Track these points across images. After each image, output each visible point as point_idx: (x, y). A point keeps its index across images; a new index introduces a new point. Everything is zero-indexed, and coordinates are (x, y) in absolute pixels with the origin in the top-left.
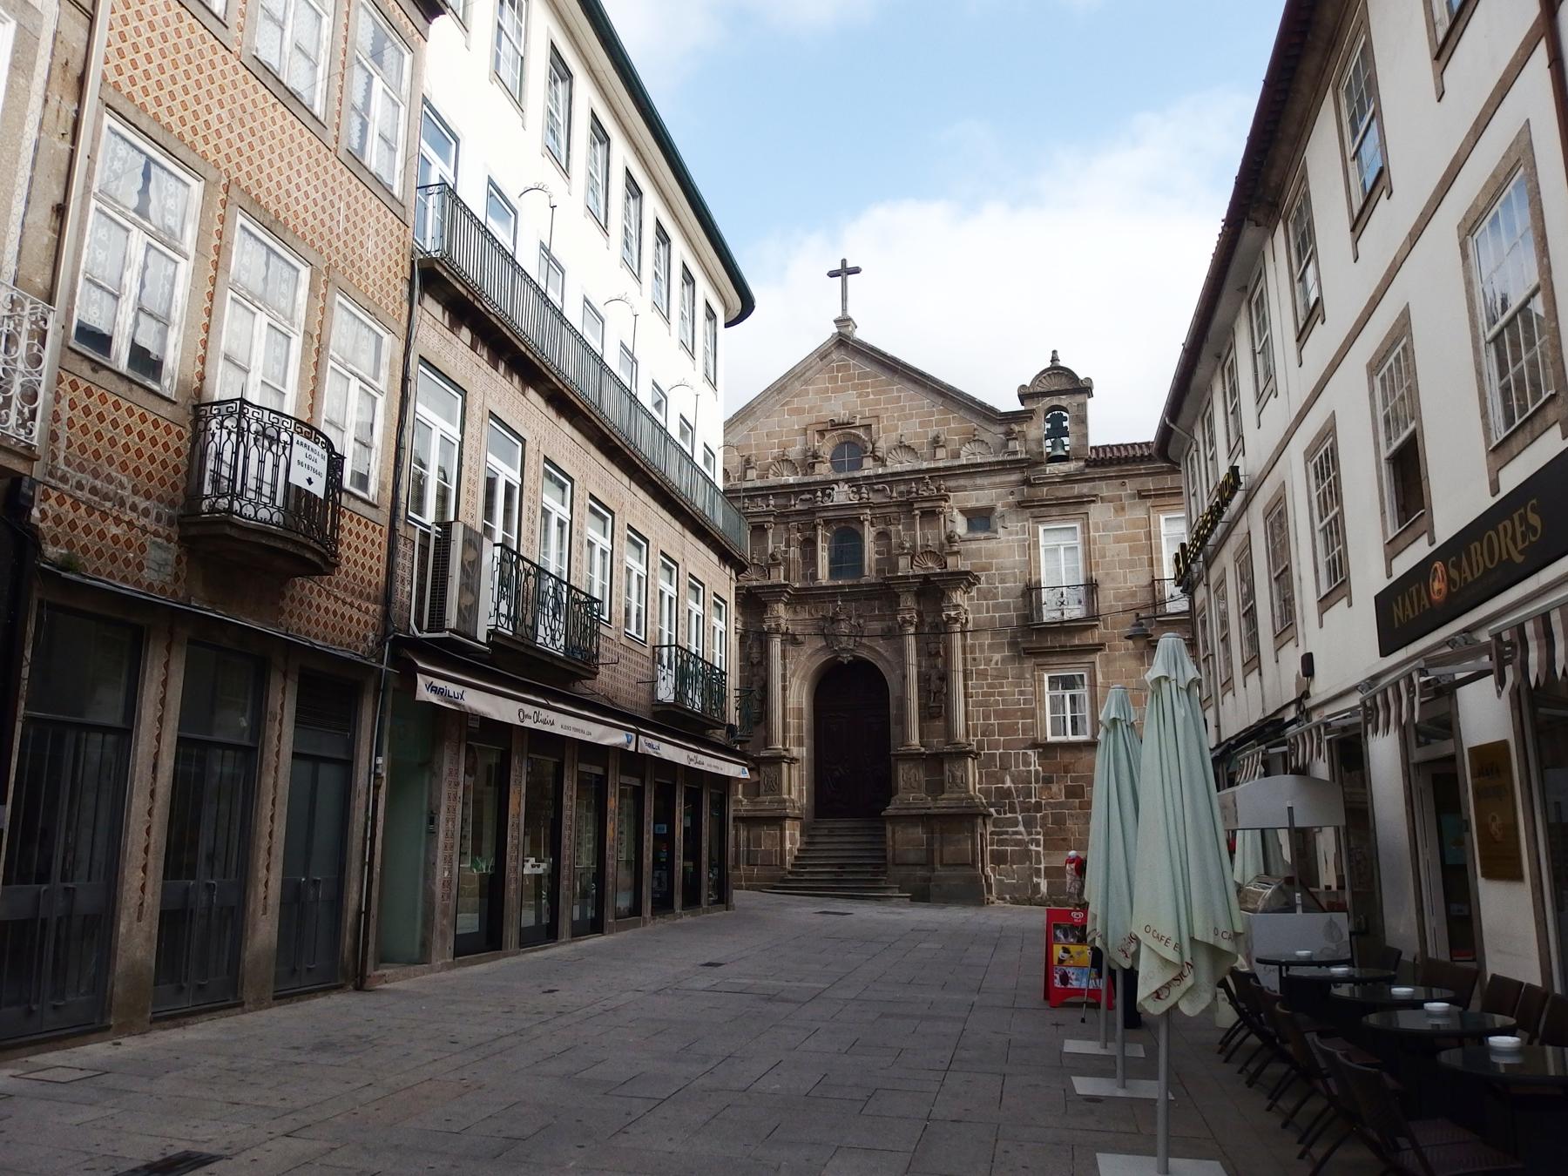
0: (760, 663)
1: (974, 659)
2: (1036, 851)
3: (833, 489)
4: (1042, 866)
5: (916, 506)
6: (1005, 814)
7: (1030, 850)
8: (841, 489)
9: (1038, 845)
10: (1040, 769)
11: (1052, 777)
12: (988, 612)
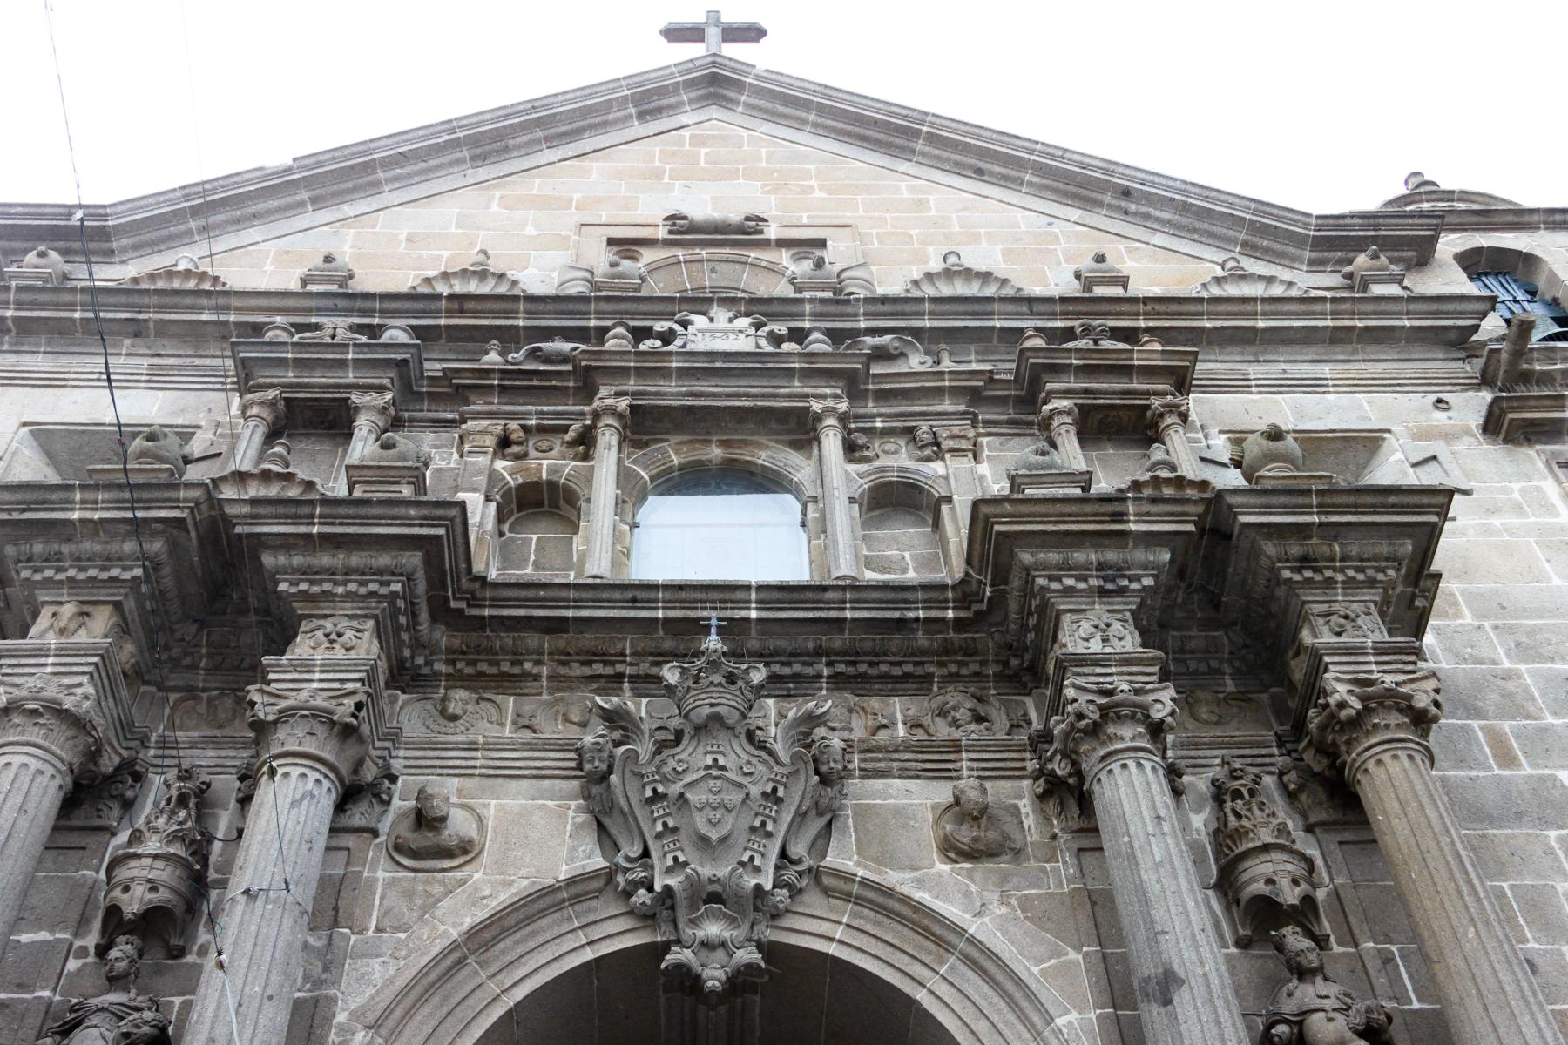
3: (685, 324)
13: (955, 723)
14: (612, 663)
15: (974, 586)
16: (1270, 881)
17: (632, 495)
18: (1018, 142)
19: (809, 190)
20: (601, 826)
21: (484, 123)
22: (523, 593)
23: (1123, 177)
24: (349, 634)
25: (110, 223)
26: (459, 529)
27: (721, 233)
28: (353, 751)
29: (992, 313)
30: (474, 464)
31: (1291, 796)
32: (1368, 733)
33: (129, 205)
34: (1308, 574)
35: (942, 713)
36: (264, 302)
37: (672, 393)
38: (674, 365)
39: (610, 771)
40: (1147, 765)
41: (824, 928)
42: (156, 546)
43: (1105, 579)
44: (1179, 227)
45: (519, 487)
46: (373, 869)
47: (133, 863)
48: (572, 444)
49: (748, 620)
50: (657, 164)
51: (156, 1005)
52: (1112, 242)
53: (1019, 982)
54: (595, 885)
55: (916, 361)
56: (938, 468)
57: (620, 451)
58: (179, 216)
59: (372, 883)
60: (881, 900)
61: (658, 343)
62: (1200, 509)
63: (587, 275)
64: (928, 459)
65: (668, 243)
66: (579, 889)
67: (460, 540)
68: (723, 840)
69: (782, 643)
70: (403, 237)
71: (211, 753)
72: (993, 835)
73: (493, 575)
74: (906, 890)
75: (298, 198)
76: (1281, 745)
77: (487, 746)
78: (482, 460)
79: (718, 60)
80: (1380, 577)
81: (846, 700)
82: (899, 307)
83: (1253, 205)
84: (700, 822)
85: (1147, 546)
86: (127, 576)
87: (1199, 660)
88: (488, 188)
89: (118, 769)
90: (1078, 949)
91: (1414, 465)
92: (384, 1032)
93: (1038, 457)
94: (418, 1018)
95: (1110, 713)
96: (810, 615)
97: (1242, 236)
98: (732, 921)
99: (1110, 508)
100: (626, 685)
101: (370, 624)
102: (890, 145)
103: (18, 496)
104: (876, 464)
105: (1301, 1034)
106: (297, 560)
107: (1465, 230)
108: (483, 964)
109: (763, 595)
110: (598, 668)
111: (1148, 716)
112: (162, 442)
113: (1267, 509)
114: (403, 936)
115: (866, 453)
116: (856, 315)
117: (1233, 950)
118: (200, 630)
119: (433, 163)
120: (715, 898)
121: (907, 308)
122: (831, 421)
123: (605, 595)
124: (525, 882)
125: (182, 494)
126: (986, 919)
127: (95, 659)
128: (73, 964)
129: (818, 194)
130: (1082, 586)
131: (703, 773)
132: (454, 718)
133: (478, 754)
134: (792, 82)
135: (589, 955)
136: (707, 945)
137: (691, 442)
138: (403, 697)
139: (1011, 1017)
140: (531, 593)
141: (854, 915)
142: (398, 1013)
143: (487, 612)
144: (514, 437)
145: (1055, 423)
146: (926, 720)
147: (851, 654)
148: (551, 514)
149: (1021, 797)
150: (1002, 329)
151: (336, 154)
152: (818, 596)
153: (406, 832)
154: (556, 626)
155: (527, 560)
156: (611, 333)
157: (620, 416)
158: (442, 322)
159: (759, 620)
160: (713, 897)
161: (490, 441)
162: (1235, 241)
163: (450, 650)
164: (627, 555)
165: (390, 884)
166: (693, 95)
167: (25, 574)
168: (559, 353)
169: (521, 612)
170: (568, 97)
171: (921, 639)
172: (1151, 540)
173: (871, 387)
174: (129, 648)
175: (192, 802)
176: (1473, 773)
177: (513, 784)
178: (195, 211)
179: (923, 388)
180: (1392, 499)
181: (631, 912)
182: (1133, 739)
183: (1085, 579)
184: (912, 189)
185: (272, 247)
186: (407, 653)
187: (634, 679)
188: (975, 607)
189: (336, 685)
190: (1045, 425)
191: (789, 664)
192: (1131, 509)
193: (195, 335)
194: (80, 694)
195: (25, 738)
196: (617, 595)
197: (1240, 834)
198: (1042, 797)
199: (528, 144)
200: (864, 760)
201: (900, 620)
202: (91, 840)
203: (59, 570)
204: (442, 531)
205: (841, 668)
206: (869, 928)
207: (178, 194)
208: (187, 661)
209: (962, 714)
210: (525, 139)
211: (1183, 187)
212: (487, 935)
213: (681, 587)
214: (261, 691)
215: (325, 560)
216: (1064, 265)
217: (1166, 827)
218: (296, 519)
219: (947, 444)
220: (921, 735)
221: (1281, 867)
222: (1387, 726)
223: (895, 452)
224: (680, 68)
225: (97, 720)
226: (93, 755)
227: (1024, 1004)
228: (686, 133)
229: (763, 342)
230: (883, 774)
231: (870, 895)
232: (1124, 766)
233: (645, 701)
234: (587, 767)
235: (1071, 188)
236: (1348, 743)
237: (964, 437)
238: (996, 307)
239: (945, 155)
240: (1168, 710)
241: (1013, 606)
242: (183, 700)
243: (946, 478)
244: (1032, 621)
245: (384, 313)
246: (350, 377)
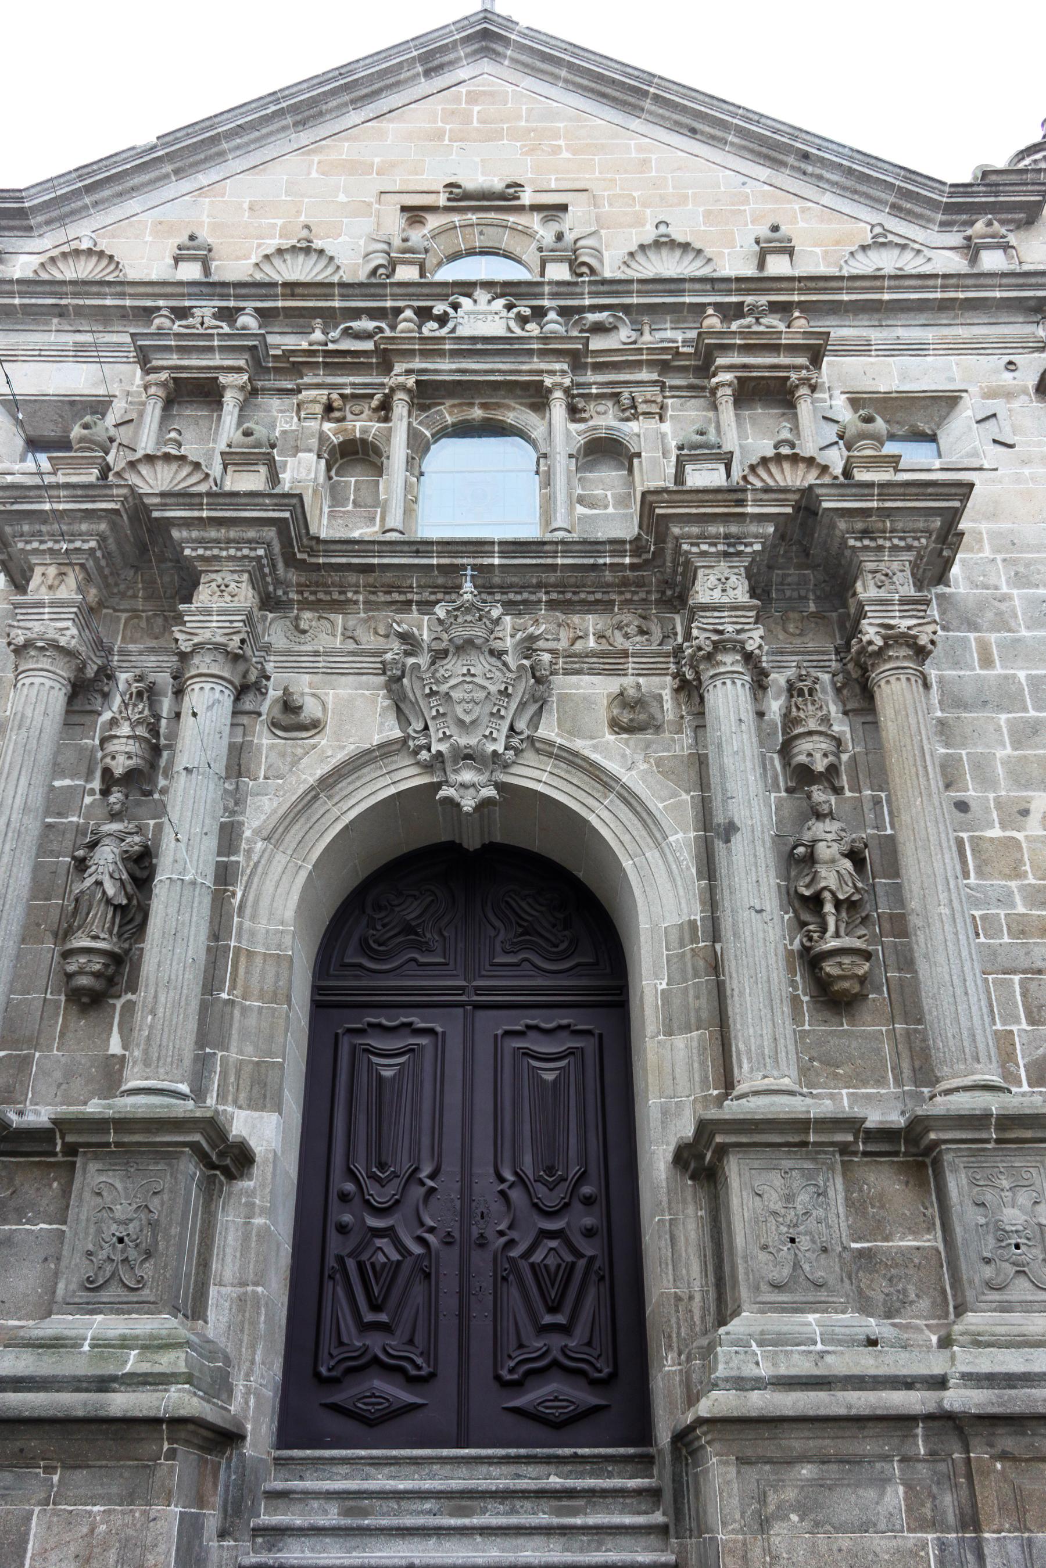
0: (131, 777)
1: (962, 806)
3: (456, 306)
5: (720, 361)
8: (482, 306)
12: (987, 661)
13: (627, 636)
14: (405, 593)
15: (644, 543)
16: (810, 755)
17: (419, 447)
18: (725, 106)
19: (556, 150)
20: (398, 707)
21: (301, 92)
22: (344, 547)
23: (805, 142)
24: (233, 585)
25: (26, 205)
26: (299, 510)
27: (488, 200)
28: (241, 667)
29: (684, 291)
30: (308, 428)
31: (838, 691)
32: (885, 661)
33: (39, 188)
34: (866, 542)
35: (619, 628)
36: (149, 290)
37: (445, 368)
38: (447, 347)
39: (403, 676)
40: (739, 683)
41: (536, 774)
42: (103, 526)
43: (729, 545)
44: (845, 188)
45: (341, 444)
46: (260, 737)
47: (116, 741)
48: (376, 410)
49: (492, 565)
50: (440, 124)
51: (140, 830)
52: (789, 202)
53: (650, 813)
54: (395, 747)
55: (624, 334)
56: (633, 426)
57: (409, 416)
58: (76, 194)
59: (259, 747)
60: (571, 758)
61: (436, 325)
62: (796, 497)
63: (385, 247)
64: (627, 420)
65: (448, 209)
66: (386, 750)
67: (300, 516)
68: (473, 722)
69: (515, 580)
70: (246, 206)
71: (153, 658)
72: (643, 717)
73: (323, 535)
74: (586, 752)
75: (164, 171)
76: (837, 653)
77: (326, 654)
78: (313, 425)
79: (489, 15)
80: (916, 543)
81: (557, 618)
82: (615, 288)
83: (903, 173)
84: (459, 710)
85: (759, 522)
86: (86, 546)
87: (793, 590)
88: (308, 153)
89: (97, 673)
90: (688, 792)
91: (978, 422)
92: (273, 841)
93: (699, 437)
94: (293, 831)
95: (719, 647)
96: (534, 561)
97: (892, 199)
98: (479, 771)
99: (735, 496)
100: (414, 607)
101: (246, 576)
102: (625, 103)
103: (8, 493)
104: (591, 423)
105: (812, 853)
106: (195, 534)
108: (329, 797)
109: (504, 548)
110: (396, 596)
111: (743, 648)
112: (94, 430)
113: (842, 497)
114: (280, 781)
115: (583, 415)
116: (582, 294)
117: (784, 794)
118: (136, 573)
119: (264, 131)
120: (468, 757)
121: (620, 288)
122: (558, 394)
123: (398, 548)
124: (353, 747)
125: (115, 491)
126: (634, 773)
127: (75, 610)
128: (88, 800)
129: (566, 155)
130: (713, 550)
131: (461, 679)
132: (304, 632)
133: (320, 659)
134: (548, 40)
135: (393, 790)
136: (463, 786)
137: (460, 405)
138: (270, 616)
139: (644, 833)
140: (349, 547)
141: (555, 766)
142: (281, 830)
143: (321, 560)
144: (335, 404)
145: (719, 393)
146: (608, 633)
147: (561, 586)
148: (363, 461)
149: (664, 688)
150: (691, 304)
151: (190, 130)
152: (539, 548)
153: (277, 712)
154: (367, 569)
155: (348, 499)
156: (402, 316)
157: (409, 391)
158: (280, 304)
159: (500, 565)
160: (468, 757)
161: (318, 409)
162: (886, 203)
163: (299, 585)
164: (415, 501)
165: (272, 747)
166: (469, 50)
167: (20, 545)
168: (365, 331)
169: (344, 560)
170: (367, 61)
171: (608, 576)
173: (589, 360)
174: (93, 591)
175: (146, 695)
176: (962, 673)
177: (343, 678)
178: (89, 189)
179: (627, 361)
180: (930, 490)
181: (418, 763)
182: (732, 664)
183: (715, 545)
184: (640, 149)
185: (148, 217)
186: (271, 588)
187: (419, 603)
188: (644, 556)
189: (227, 624)
190: (713, 391)
191: (520, 593)
192: (749, 497)
193: (103, 316)
194: (69, 635)
195: (40, 666)
196: (406, 548)
197: (797, 721)
198: (677, 691)
199: (338, 107)
200: (565, 663)
201: (593, 565)
202: (87, 719)
203: (42, 542)
204: (287, 515)
205: (554, 596)
206: (563, 774)
207: (74, 175)
208: (130, 593)
209: (632, 630)
210: (334, 103)
211: (850, 153)
212: (331, 780)
213: (448, 543)
214: (181, 631)
215: (213, 534)
216: (750, 226)
217: (744, 727)
218: (191, 507)
219: (642, 408)
220: (605, 646)
221: (818, 746)
222: (897, 657)
223: (605, 413)
224: (458, 25)
225: (82, 649)
226: (81, 669)
227: (652, 826)
228: (462, 89)
229: (513, 324)
230: (578, 672)
231: (565, 754)
232: (724, 683)
233: (426, 617)
234: (389, 673)
235: (764, 150)
236: (873, 665)
237: (654, 402)
238: (687, 286)
239: (667, 114)
240: (756, 645)
241: (669, 558)
243: (639, 436)
244: (680, 569)
245: (237, 297)
246: (217, 360)
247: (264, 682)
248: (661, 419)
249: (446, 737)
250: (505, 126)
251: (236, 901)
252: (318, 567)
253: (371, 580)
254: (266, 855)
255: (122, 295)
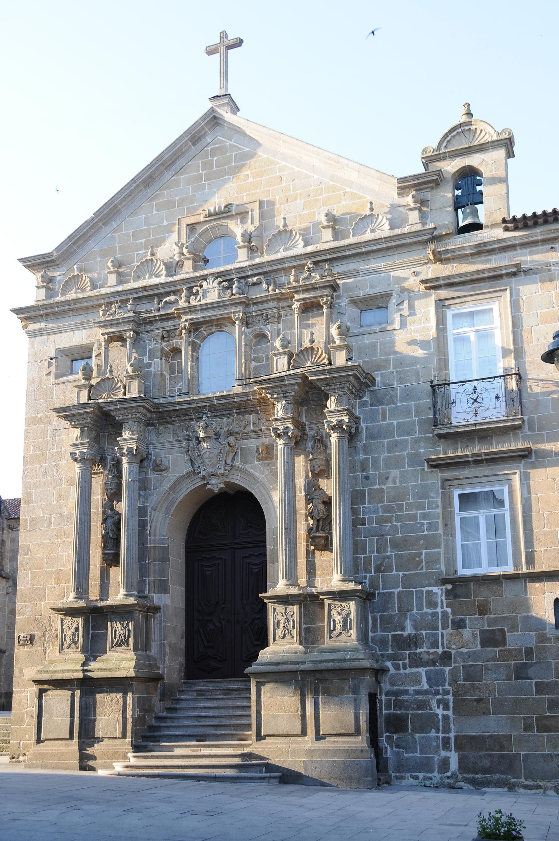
1: (367, 478)
2: (443, 715)
3: (201, 286)
4: (452, 735)
6: (405, 668)
7: (437, 715)
9: (446, 707)
10: (449, 610)
11: (463, 621)
17: (195, 347)
34: (328, 388)
37: (198, 316)
39: (189, 451)
50: (201, 172)
58: (70, 247)
64: (267, 325)
70: (131, 234)
74: (249, 469)
107: (462, 155)
110: (187, 417)
120: (213, 475)
135: (193, 488)
143: (161, 410)
172: (292, 384)
187: (195, 418)
199: (160, 173)
205: (238, 411)
215: (123, 412)
230: (247, 439)
242: (108, 435)
247: (149, 456)
248: (279, 323)
249: (204, 470)
250: (226, 167)
251: (148, 532)
252: (161, 412)
253: (178, 413)
254: (156, 515)
255: (89, 301)
